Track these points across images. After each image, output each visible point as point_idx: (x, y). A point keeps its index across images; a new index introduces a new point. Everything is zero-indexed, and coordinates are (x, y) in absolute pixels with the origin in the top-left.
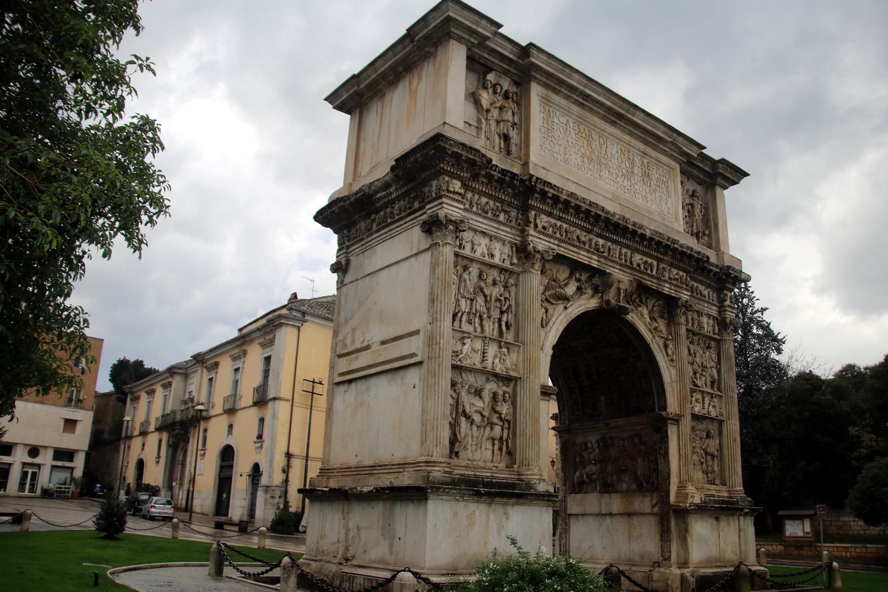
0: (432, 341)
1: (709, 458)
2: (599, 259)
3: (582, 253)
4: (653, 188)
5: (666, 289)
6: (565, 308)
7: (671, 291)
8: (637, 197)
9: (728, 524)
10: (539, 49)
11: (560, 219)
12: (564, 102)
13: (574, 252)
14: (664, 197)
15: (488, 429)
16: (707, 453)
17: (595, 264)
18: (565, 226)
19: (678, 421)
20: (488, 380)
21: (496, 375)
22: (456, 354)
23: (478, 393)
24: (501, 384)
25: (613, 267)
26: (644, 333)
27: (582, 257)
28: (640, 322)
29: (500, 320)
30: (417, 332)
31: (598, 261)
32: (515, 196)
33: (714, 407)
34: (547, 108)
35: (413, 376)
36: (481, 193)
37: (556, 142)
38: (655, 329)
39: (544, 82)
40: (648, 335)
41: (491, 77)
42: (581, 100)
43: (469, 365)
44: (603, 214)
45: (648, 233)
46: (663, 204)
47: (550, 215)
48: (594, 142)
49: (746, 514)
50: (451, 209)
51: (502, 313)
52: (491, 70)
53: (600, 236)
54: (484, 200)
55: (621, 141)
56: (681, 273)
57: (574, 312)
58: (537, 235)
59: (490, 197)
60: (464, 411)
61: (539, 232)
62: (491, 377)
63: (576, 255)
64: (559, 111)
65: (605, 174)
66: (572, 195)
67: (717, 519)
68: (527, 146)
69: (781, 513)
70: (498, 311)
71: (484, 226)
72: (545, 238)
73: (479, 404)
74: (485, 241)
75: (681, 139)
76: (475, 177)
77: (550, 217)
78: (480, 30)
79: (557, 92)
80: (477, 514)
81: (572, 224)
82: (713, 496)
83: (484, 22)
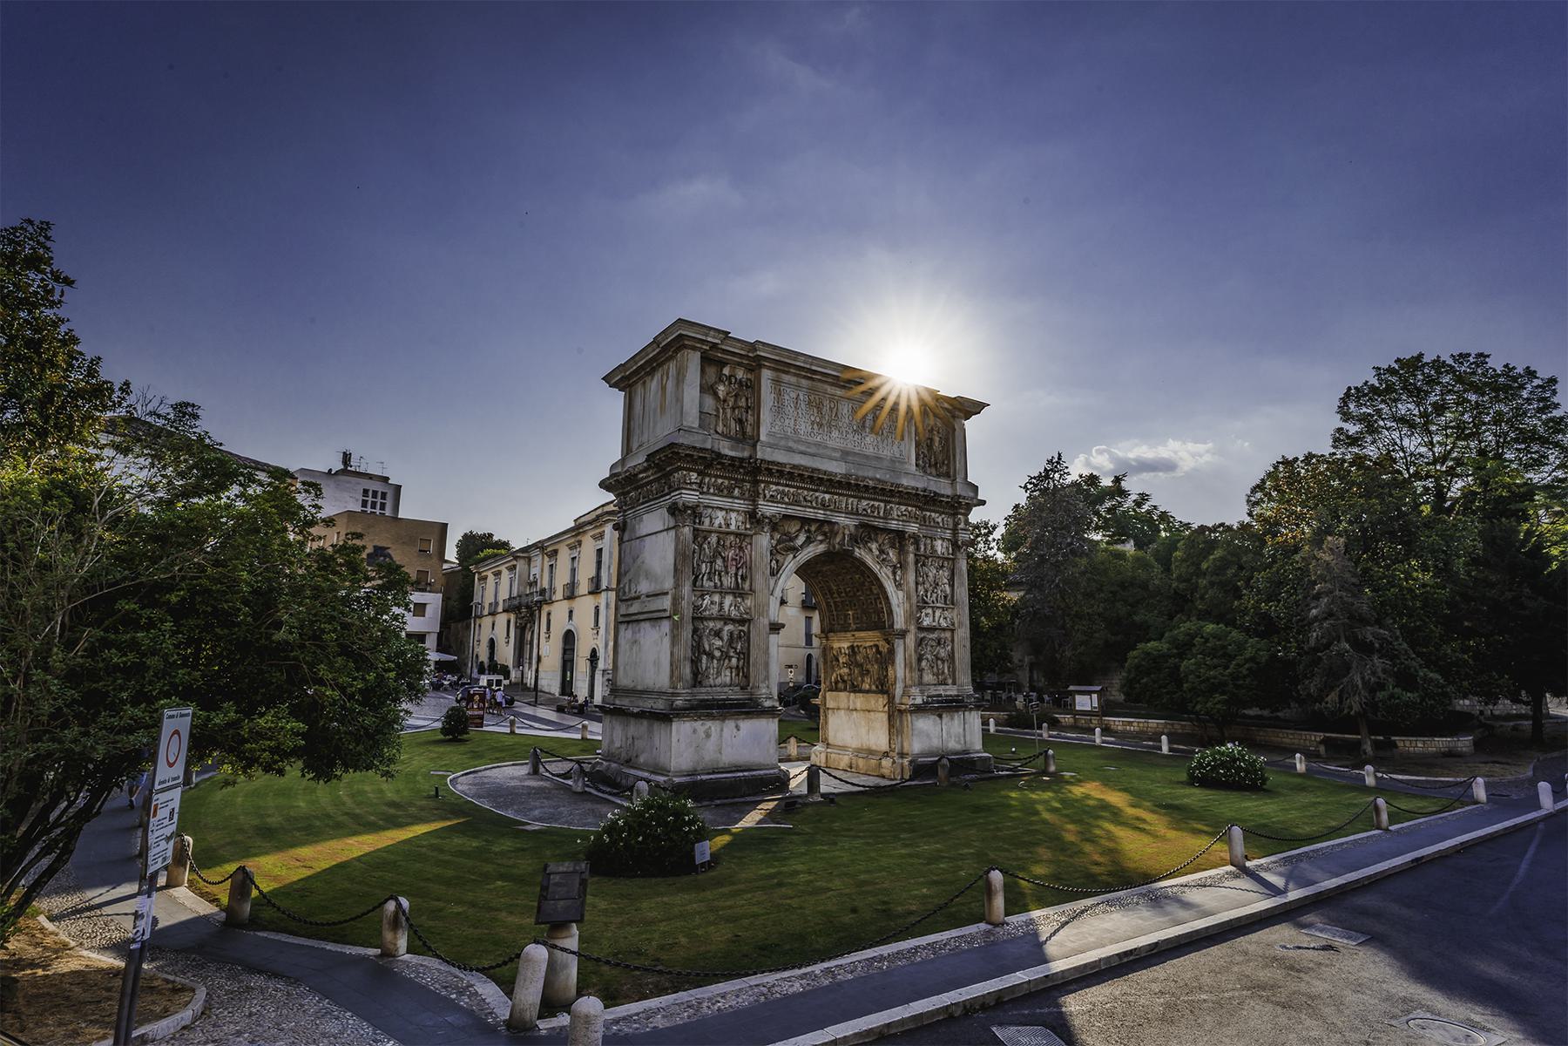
0: (676, 601)
1: (939, 662)
5: (893, 525)
6: (795, 557)
9: (952, 719)
10: (764, 344)
11: (787, 486)
12: (793, 379)
15: (727, 661)
16: (937, 659)
17: (821, 517)
18: (792, 490)
20: (725, 624)
21: (732, 620)
22: (696, 608)
23: (718, 634)
29: (736, 574)
30: (667, 593)
32: (746, 474)
33: (945, 618)
35: (666, 626)
36: (717, 477)
37: (785, 417)
38: (883, 560)
41: (726, 371)
46: (895, 447)
47: (777, 484)
49: (971, 710)
50: (689, 497)
51: (738, 569)
53: (826, 493)
54: (720, 481)
56: (910, 508)
59: (725, 478)
60: (704, 651)
61: (768, 501)
65: (835, 434)
66: (794, 467)
67: (940, 716)
68: (759, 428)
69: (1071, 688)
70: (734, 568)
73: (718, 643)
74: (721, 514)
76: (709, 466)
78: (709, 339)
79: (787, 373)
81: (798, 488)
82: (940, 695)
83: (712, 333)
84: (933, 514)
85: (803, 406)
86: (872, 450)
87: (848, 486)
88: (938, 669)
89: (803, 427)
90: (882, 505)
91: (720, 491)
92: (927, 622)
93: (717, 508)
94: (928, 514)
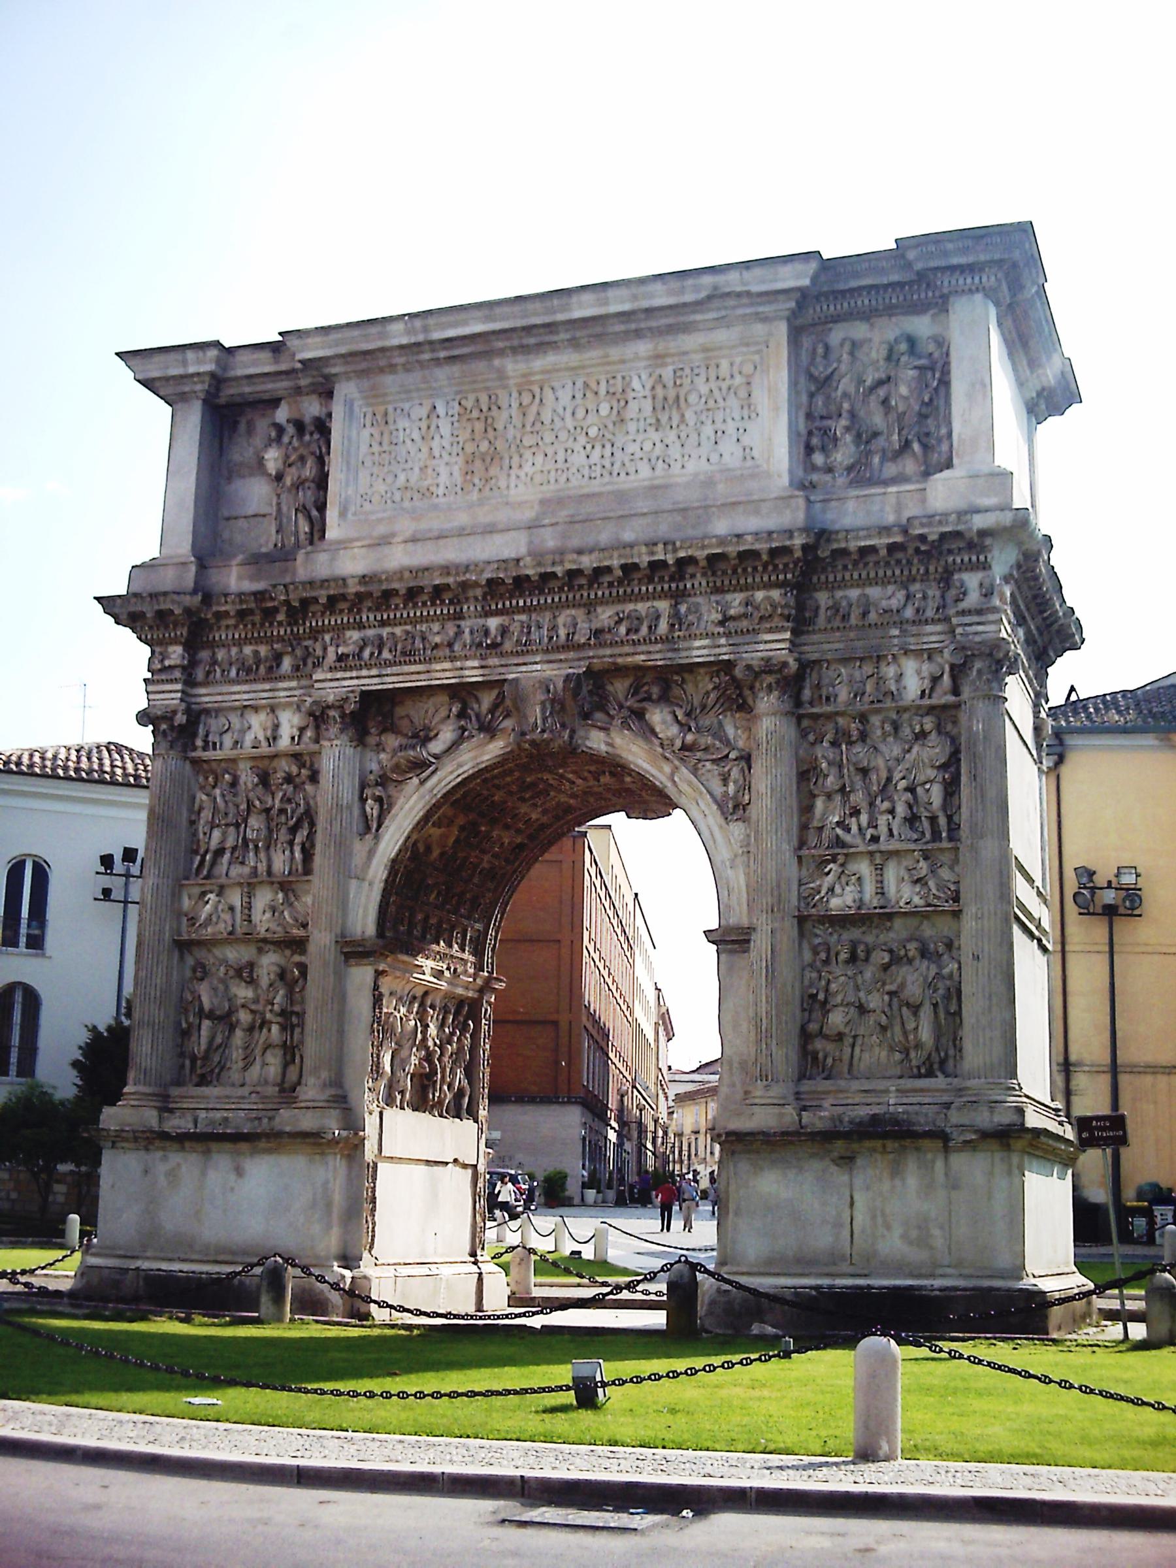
2: (484, 663)
3: (438, 667)
4: (691, 423)
7: (717, 651)
8: (632, 470)
9: (896, 1171)
11: (383, 623)
13: (418, 673)
14: (731, 427)
15: (265, 1030)
18: (398, 631)
19: (748, 941)
20: (260, 951)
23: (246, 973)
24: (288, 952)
25: (525, 664)
26: (646, 766)
27: (438, 675)
28: (634, 749)
31: (482, 667)
34: (382, 409)
36: (240, 643)
39: (355, 372)
40: (661, 770)
41: (282, 414)
42: (442, 354)
43: (214, 934)
44: (450, 580)
45: (587, 562)
47: (361, 626)
48: (504, 415)
52: (275, 402)
54: (248, 650)
55: (583, 367)
56: (760, 595)
57: (443, 784)
58: (329, 676)
59: (259, 641)
60: (201, 1008)
62: (261, 944)
63: (422, 677)
64: (408, 400)
70: (283, 830)
71: (246, 696)
72: (348, 674)
73: (243, 993)
75: (733, 276)
77: (364, 627)
79: (392, 368)
80: (184, 1168)
84: (874, 592)
85: (445, 430)
86: (645, 471)
87: (521, 584)
88: (905, 1033)
89: (443, 479)
90: (663, 606)
91: (249, 672)
92: (841, 901)
93: (245, 707)
94: (854, 593)
